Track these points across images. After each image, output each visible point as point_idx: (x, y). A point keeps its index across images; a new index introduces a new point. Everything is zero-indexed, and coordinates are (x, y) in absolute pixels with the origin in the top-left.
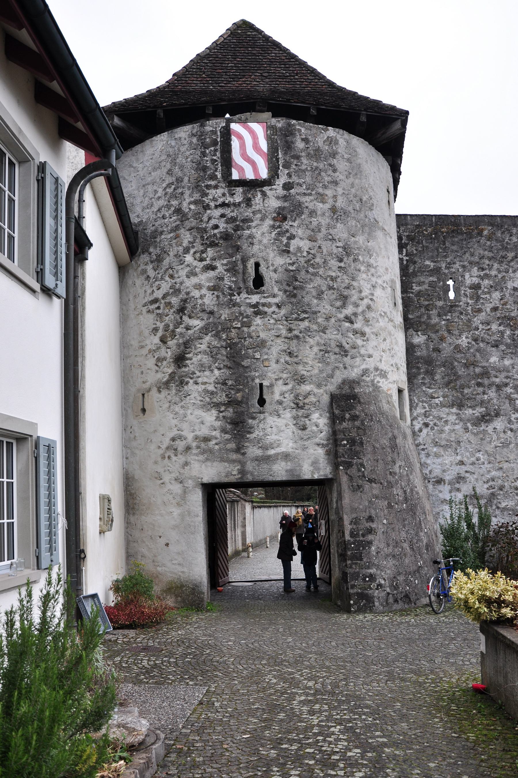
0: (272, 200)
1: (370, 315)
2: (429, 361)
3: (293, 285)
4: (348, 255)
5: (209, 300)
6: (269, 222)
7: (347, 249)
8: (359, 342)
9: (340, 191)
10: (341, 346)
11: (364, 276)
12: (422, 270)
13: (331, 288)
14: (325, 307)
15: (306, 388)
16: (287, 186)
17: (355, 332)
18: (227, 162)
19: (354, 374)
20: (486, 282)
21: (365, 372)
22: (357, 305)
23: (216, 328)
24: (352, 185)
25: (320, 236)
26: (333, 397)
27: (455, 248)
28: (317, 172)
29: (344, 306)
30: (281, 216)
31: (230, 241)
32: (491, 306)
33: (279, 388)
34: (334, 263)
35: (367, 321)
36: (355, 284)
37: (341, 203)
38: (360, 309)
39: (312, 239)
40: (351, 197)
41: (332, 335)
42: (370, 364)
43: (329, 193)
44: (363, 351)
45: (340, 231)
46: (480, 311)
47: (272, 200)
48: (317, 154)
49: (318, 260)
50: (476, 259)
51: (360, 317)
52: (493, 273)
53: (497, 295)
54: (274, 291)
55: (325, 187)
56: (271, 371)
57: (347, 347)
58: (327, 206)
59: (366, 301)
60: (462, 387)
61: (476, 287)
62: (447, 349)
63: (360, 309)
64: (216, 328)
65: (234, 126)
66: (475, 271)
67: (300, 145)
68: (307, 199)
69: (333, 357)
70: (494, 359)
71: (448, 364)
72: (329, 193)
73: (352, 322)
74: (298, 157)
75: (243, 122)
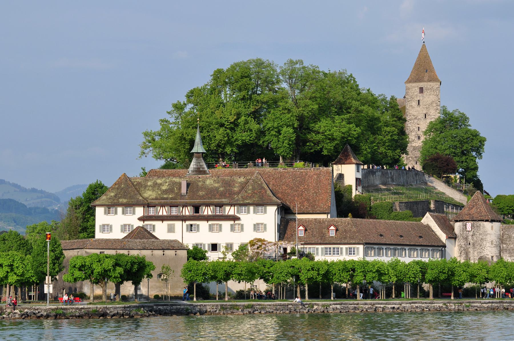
0: (471, 233)
3: (474, 244)
5: (464, 246)
7: (482, 239)
12: (506, 234)
28: (477, 229)
30: (472, 236)
31: (466, 239)
45: (481, 237)
48: (478, 227)
56: (471, 255)
62: (509, 247)
71: (509, 250)
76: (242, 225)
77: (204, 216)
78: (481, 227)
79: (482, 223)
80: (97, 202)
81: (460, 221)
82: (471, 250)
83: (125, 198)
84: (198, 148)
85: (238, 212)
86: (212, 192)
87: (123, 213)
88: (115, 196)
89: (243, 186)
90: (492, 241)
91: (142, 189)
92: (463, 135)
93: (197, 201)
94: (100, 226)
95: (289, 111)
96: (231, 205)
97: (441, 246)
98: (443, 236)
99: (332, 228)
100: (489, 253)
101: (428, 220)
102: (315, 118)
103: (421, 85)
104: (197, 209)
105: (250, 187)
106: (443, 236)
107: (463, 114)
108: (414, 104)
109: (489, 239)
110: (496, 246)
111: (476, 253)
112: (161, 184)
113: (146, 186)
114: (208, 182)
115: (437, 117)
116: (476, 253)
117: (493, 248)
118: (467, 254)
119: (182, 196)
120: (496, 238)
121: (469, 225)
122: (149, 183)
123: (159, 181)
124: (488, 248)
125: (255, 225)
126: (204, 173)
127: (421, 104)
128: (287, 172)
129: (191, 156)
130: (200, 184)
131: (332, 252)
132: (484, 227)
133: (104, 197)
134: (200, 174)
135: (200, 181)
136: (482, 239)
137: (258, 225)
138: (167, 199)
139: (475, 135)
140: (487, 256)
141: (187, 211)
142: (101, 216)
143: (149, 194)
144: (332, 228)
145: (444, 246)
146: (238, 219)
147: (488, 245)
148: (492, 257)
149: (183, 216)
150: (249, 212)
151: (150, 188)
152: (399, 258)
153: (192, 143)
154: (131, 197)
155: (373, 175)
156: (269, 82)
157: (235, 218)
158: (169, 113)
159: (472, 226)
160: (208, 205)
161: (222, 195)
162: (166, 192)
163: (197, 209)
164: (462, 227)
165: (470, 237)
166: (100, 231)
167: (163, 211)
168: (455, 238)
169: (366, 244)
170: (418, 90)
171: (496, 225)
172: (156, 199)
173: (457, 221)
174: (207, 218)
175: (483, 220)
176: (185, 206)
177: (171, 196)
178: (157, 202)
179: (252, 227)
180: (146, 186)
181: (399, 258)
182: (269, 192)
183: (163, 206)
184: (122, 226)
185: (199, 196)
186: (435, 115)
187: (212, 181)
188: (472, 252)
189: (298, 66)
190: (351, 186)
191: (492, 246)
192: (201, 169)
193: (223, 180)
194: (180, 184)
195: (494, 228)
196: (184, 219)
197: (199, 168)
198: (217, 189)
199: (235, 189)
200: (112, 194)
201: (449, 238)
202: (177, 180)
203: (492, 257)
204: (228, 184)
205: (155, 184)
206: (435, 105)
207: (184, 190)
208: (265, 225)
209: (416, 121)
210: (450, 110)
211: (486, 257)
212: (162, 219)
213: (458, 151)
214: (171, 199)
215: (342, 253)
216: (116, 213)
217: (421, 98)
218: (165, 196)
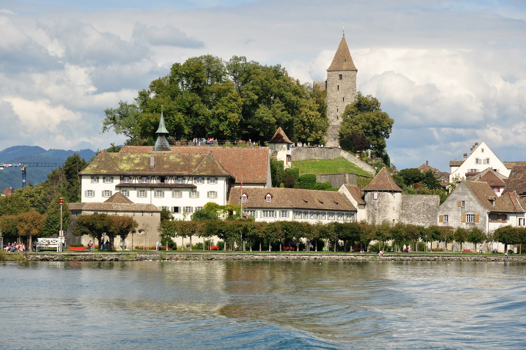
0: (377, 201)
3: (379, 210)
23: (372, 214)
45: (385, 204)
47: (377, 201)
54: (377, 211)
64: (372, 214)
71: (407, 215)
76: (198, 192)
77: (168, 185)
79: (386, 193)
80: (83, 172)
81: (369, 191)
82: (377, 214)
83: (105, 170)
84: (162, 129)
85: (195, 182)
86: (175, 165)
87: (104, 181)
88: (98, 167)
89: (199, 161)
90: (394, 208)
91: (119, 162)
92: (375, 117)
93: (163, 173)
94: (85, 191)
95: (235, 100)
96: (190, 176)
97: (353, 211)
98: (355, 204)
99: (269, 195)
100: (391, 217)
101: (344, 190)
102: (255, 106)
103: (340, 73)
104: (162, 178)
105: (205, 163)
106: (355, 204)
107: (375, 99)
108: (335, 88)
111: (380, 217)
112: (133, 159)
113: (122, 160)
114: (171, 157)
115: (353, 101)
116: (380, 217)
118: (374, 217)
119: (150, 169)
120: (397, 205)
121: (376, 194)
122: (124, 158)
123: (132, 156)
125: (208, 192)
126: (167, 149)
127: (340, 88)
128: (233, 150)
129: (155, 135)
130: (165, 159)
131: (268, 215)
132: (388, 196)
133: (88, 168)
134: (163, 150)
135: (165, 157)
137: (211, 193)
138: (138, 170)
139: (384, 116)
141: (155, 182)
142: (86, 184)
143: (125, 167)
144: (269, 195)
145: (356, 211)
146: (195, 187)
148: (394, 220)
149: (152, 184)
150: (203, 183)
151: (125, 162)
152: (321, 220)
153: (156, 125)
154: (110, 169)
155: (300, 152)
156: (217, 76)
157: (192, 188)
158: (136, 99)
160: (171, 176)
161: (183, 168)
162: (138, 165)
163: (162, 178)
164: (370, 196)
165: (376, 204)
166: (86, 196)
167: (135, 181)
168: (365, 205)
169: (295, 208)
170: (338, 77)
171: (398, 195)
172: (130, 170)
173: (366, 191)
174: (170, 187)
176: (153, 177)
177: (142, 168)
178: (131, 173)
179: (206, 194)
180: (122, 160)
181: (321, 220)
182: (219, 166)
183: (135, 176)
184: (103, 192)
185: (165, 169)
186: (351, 100)
187: (174, 157)
189: (241, 62)
190: (283, 161)
192: (164, 147)
193: (183, 156)
194: (149, 159)
196: (152, 187)
197: (162, 146)
198: (178, 164)
199: (193, 163)
200: (95, 166)
201: (360, 204)
202: (147, 155)
204: (187, 159)
205: (129, 159)
206: (351, 90)
207: (152, 164)
208: (216, 192)
209: (335, 103)
210: (364, 95)
212: (135, 187)
213: (371, 131)
214: (142, 170)
215: (276, 216)
216: (98, 181)
217: (340, 85)
218: (137, 168)
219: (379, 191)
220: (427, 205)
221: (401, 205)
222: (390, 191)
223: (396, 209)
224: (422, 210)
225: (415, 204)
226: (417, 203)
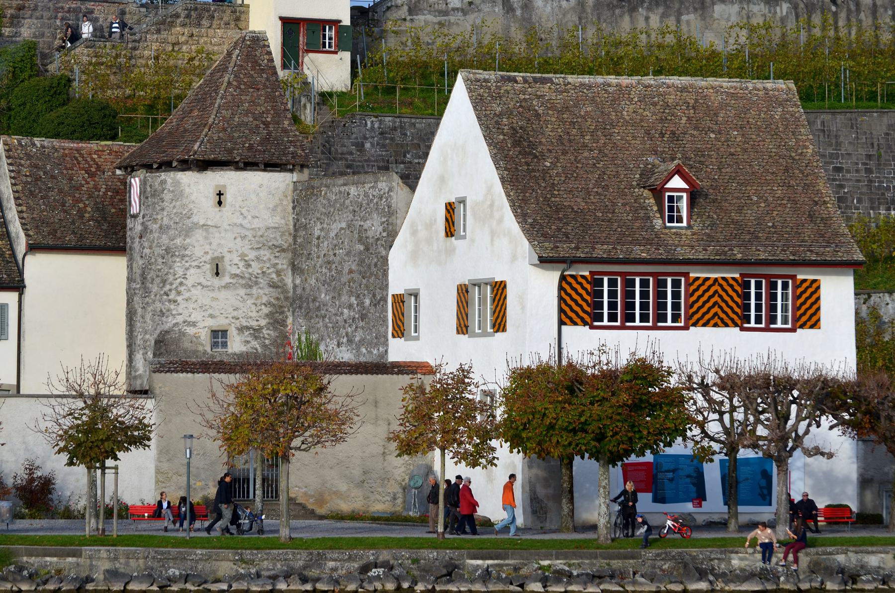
1: (182, 288)
2: (301, 298)
4: (168, 253)
6: (137, 240)
7: (168, 250)
8: (172, 307)
9: (165, 213)
10: (161, 311)
11: (179, 264)
13: (158, 276)
14: (155, 289)
15: (147, 336)
16: (143, 218)
17: (170, 301)
18: (130, 202)
19: (166, 327)
20: (323, 233)
21: (176, 324)
22: (171, 284)
24: (174, 207)
25: (154, 244)
26: (158, 342)
27: (312, 207)
29: (164, 286)
32: (323, 253)
33: (139, 337)
34: (160, 260)
35: (179, 293)
36: (171, 271)
37: (166, 221)
38: (174, 286)
39: (151, 248)
40: (172, 216)
41: (158, 305)
42: (180, 319)
43: (159, 217)
44: (174, 312)
45: (165, 240)
46: (318, 257)
49: (153, 260)
50: (318, 215)
51: (174, 292)
52: (325, 226)
53: (326, 243)
55: (157, 214)
57: (164, 311)
58: (158, 225)
59: (179, 280)
60: (311, 318)
61: (318, 238)
63: (174, 286)
65: (132, 180)
66: (319, 226)
67: (149, 189)
68: (149, 223)
69: (157, 318)
70: (323, 295)
72: (159, 217)
73: (168, 295)
74: (147, 198)
75: (134, 177)
78: (167, 196)
79: (169, 177)
100: (196, 316)
109: (198, 252)
110: (250, 283)
111: (148, 316)
116: (148, 316)
117: (224, 294)
120: (244, 247)
124: (197, 292)
132: (178, 195)
136: (168, 250)
140: (191, 331)
145: (18, 286)
147: (194, 276)
159: (143, 192)
165: (136, 245)
175: (166, 165)
188: (140, 310)
191: (217, 282)
195: (228, 198)
203: (219, 336)
211: (183, 334)
219: (148, 167)
220: (360, 240)
221: (285, 241)
222: (186, 165)
223: (232, 265)
224: (346, 270)
225: (326, 238)
226: (335, 227)
